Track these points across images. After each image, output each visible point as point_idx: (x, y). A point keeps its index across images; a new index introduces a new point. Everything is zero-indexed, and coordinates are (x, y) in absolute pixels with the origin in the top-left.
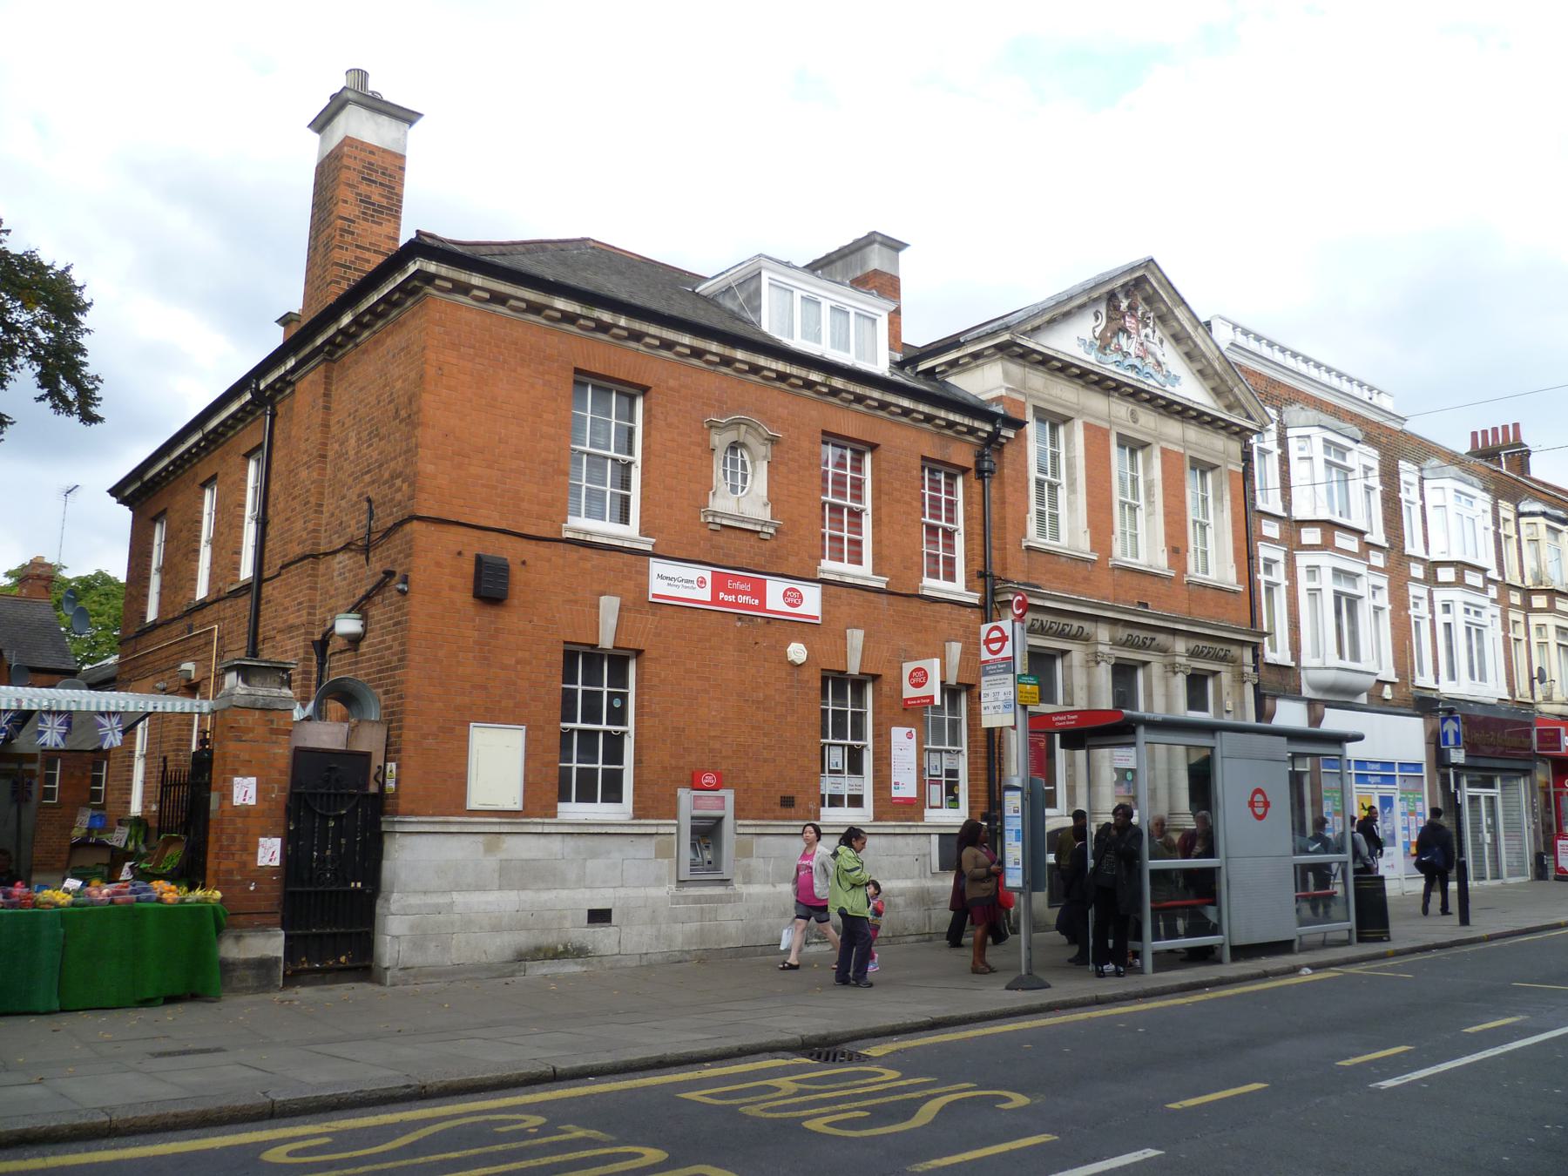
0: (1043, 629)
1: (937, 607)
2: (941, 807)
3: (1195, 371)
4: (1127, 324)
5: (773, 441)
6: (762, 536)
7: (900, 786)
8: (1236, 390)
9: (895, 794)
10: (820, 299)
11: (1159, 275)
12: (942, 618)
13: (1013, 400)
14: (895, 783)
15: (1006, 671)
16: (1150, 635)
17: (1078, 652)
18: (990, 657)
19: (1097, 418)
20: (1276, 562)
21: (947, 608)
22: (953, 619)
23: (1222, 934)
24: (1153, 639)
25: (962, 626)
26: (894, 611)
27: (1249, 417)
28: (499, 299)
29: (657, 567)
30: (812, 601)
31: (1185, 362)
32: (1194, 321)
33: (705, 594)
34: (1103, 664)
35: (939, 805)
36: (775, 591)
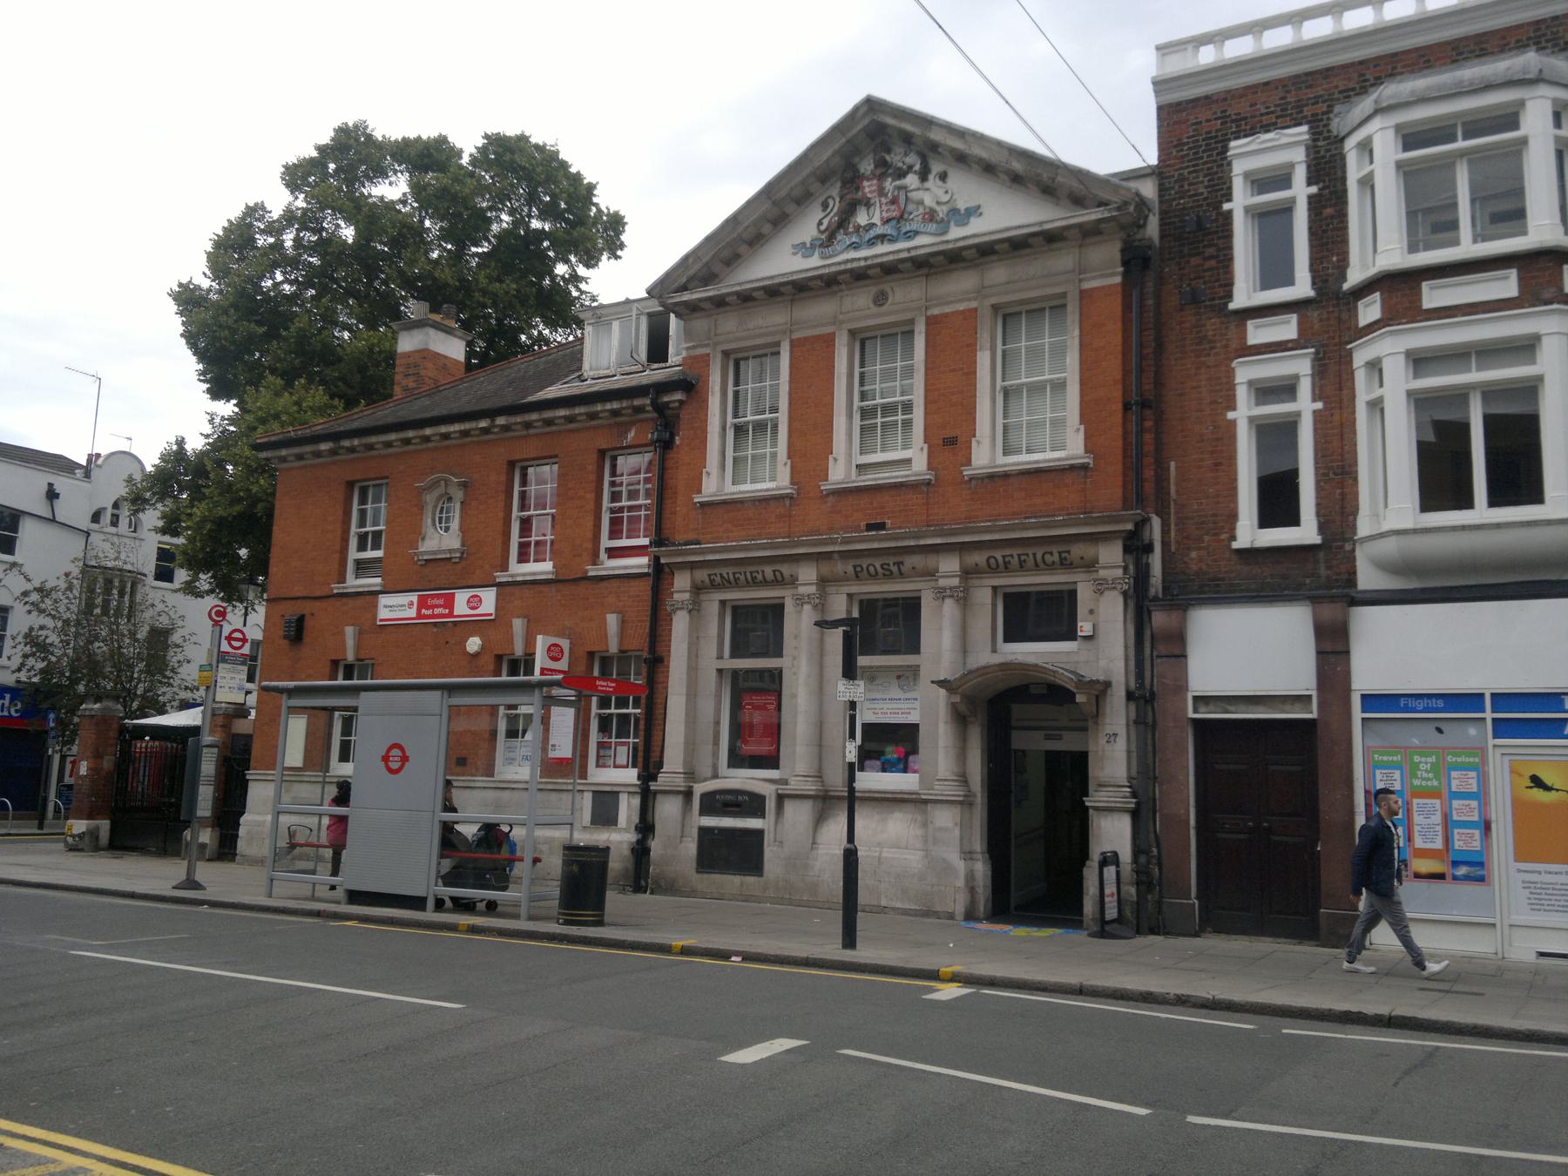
1: (605, 584)
2: (627, 767)
5: (464, 485)
6: (454, 560)
13: (695, 357)
14: (553, 746)
15: (243, 663)
18: (230, 650)
21: (615, 583)
27: (1102, 204)
29: (384, 600)
30: (488, 600)
33: (412, 613)
35: (625, 763)
36: (461, 599)
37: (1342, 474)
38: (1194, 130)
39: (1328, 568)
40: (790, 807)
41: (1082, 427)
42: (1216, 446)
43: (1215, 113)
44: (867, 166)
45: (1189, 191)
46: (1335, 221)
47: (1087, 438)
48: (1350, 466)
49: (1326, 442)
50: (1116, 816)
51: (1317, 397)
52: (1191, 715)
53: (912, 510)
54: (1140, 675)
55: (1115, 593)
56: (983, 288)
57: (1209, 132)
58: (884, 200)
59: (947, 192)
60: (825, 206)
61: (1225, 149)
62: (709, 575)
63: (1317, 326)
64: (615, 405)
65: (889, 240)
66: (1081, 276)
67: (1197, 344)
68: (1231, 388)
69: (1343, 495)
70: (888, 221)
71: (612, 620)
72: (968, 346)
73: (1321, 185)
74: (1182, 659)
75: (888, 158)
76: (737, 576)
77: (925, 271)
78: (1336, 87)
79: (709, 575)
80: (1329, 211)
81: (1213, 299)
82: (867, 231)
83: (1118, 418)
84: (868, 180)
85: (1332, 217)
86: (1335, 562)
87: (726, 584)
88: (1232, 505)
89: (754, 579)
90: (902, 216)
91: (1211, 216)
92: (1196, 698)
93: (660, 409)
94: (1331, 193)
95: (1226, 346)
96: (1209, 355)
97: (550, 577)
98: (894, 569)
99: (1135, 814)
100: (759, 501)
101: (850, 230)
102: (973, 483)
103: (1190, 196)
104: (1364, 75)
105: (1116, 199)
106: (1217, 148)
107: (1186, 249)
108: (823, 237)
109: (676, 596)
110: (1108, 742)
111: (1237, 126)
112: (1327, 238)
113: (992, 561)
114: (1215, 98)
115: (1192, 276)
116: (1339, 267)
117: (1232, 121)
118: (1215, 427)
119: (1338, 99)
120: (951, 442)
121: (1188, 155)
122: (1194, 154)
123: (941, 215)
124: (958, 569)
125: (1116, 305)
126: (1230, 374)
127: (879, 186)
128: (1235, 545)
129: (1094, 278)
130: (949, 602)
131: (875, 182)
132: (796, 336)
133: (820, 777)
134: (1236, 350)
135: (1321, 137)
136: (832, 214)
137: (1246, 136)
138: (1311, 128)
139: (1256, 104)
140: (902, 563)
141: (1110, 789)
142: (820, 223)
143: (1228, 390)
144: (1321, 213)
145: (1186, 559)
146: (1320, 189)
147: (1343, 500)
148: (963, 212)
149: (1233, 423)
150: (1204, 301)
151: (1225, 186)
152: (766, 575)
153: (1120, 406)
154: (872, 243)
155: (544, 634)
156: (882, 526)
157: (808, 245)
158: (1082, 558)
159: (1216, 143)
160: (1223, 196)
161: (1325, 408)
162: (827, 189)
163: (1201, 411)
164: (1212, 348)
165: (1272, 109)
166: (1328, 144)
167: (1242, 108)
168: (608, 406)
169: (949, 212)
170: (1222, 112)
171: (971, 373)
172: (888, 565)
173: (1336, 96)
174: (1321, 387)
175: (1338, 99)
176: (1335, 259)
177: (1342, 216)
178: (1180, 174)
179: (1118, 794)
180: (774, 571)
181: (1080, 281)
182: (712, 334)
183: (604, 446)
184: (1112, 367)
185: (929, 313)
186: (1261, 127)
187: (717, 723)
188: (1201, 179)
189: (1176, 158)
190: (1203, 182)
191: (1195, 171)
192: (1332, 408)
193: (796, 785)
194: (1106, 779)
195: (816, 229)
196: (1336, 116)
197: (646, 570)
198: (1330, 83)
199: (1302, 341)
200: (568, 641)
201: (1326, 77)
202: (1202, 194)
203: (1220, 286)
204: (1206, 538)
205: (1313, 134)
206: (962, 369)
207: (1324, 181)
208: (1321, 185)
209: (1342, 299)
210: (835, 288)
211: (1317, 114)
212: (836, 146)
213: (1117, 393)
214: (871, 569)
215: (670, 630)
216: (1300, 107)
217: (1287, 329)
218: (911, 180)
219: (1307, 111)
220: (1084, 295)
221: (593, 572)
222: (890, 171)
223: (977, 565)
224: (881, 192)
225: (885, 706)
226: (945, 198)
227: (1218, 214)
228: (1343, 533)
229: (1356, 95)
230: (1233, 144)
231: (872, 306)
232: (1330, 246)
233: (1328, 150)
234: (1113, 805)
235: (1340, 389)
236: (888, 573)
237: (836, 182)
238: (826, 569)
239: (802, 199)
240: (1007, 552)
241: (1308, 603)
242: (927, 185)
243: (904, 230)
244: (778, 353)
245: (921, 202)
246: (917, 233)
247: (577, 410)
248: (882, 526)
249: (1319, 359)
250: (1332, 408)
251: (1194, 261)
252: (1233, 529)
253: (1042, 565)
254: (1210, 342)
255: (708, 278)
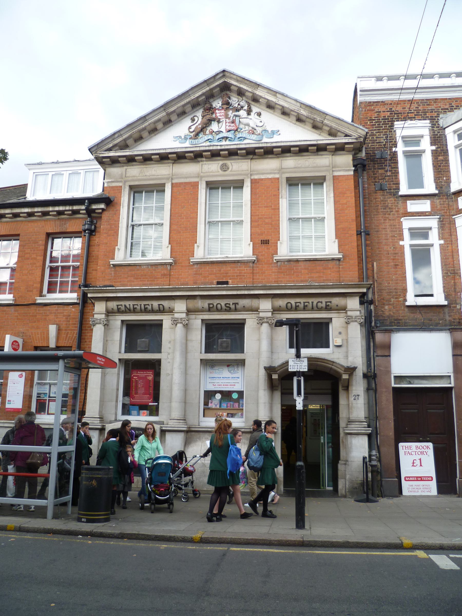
0: (130, 310)
1: (48, 308)
3: (295, 122)
4: (218, 115)
7: (12, 402)
8: (326, 121)
9: (8, 406)
10: (62, 172)
11: (235, 77)
12: (51, 313)
14: (8, 401)
16: (231, 301)
17: (167, 321)
19: (186, 178)
20: (430, 229)
21: (55, 308)
22: (58, 313)
23: (46, 499)
24: (235, 304)
25: (64, 316)
26: (18, 314)
27: (346, 136)
28: (16, 215)
31: (171, 127)
32: (272, 92)
34: (179, 325)
37: (454, 273)
38: (378, 115)
39: (450, 316)
40: (169, 436)
41: (337, 240)
42: (395, 257)
43: (387, 109)
44: (217, 104)
45: (377, 140)
46: (444, 162)
47: (340, 246)
48: (457, 270)
49: (446, 259)
50: (360, 437)
51: (441, 238)
52: (393, 385)
53: (244, 276)
54: (369, 366)
55: (356, 323)
56: (282, 168)
57: (385, 117)
58: (228, 120)
59: (261, 122)
60: (193, 120)
61: (392, 125)
62: (118, 306)
63: (439, 207)
64: (61, 208)
65: (229, 140)
66: (333, 169)
67: (384, 209)
68: (401, 230)
69: (455, 283)
70: (229, 131)
71: (53, 329)
72: (274, 195)
73: (437, 146)
74: (388, 357)
75: (229, 101)
76: (135, 306)
77: (251, 156)
78: (440, 107)
79: (118, 306)
80: (441, 158)
81: (391, 189)
82: (217, 134)
83: (355, 237)
84: (218, 109)
85: (442, 160)
86: (452, 314)
87: (128, 311)
88: (404, 285)
89: (146, 309)
90: (237, 130)
91: (387, 153)
92: (395, 377)
93: (90, 212)
94: (441, 150)
95: (398, 211)
96: (390, 214)
97: (11, 302)
98: (233, 307)
99: (370, 436)
100: (151, 265)
101: (207, 133)
102: (279, 263)
103: (377, 143)
104: (451, 104)
105: (355, 135)
106: (389, 124)
107: (376, 165)
108: (192, 134)
109: (96, 316)
110: (355, 399)
111: (397, 116)
112: (441, 169)
113: (289, 305)
114: (386, 102)
115: (380, 178)
116: (446, 182)
117: (395, 114)
118: (394, 248)
119: (441, 112)
120: (265, 242)
121: (375, 125)
122: (378, 125)
123: (259, 132)
124: (270, 308)
125: (351, 183)
126: (401, 224)
127: (225, 115)
128: (407, 304)
129: (340, 171)
130: (265, 326)
131: (223, 111)
132: (174, 181)
133: (185, 420)
134: (402, 214)
135: (435, 126)
136: (197, 124)
137: (401, 121)
138: (431, 122)
139: (405, 108)
140: (238, 304)
141: (357, 423)
142: (190, 128)
143: (400, 231)
144: (437, 158)
145: (382, 309)
146: (436, 148)
147: (455, 285)
148: (270, 132)
149: (403, 247)
150: (386, 190)
151: (393, 141)
152: (153, 306)
153: (355, 232)
154: (220, 139)
155: (11, 334)
156: (227, 283)
157: (183, 137)
158: (337, 306)
159: (388, 121)
160: (392, 144)
161: (445, 244)
162: (194, 112)
163: (387, 240)
164: (391, 212)
165: (413, 111)
166: (439, 130)
167: (399, 109)
168: (57, 208)
169: (262, 131)
170: (390, 109)
171: (277, 209)
172: (229, 304)
173: (440, 111)
174: (442, 234)
175: (441, 112)
176: (445, 178)
177: (447, 161)
178: (371, 133)
179: (360, 426)
180: (159, 305)
181: (333, 171)
182: (124, 176)
183: (50, 231)
184: (351, 213)
185: (252, 177)
186: (408, 118)
187: (118, 390)
188: (382, 136)
189: (369, 125)
190: (383, 137)
191: (378, 132)
192: (448, 244)
193: (172, 425)
194: (354, 418)
195: (188, 131)
196: (441, 118)
197: (76, 301)
198: (437, 105)
199: (432, 213)
200: (22, 340)
201: (435, 102)
202: (383, 142)
203: (393, 184)
204: (392, 300)
205: (432, 124)
206: (271, 206)
207: (438, 145)
208: (437, 146)
209: (449, 196)
210: (199, 159)
211: (433, 117)
212: (204, 91)
213: (354, 226)
214: (219, 306)
215: (92, 336)
216: (425, 113)
217: (426, 206)
218: (243, 113)
219: (428, 115)
220: (335, 178)
221: (40, 300)
222: (231, 107)
223: (280, 306)
224: (227, 117)
225: (220, 381)
226: (261, 124)
227: (390, 152)
228: (456, 301)
229: (448, 111)
230: (396, 123)
231: (220, 170)
232: (442, 173)
233: (439, 132)
234: (360, 431)
235: (451, 235)
236: (228, 309)
237: (201, 108)
238: (193, 304)
239: (182, 114)
240: (298, 300)
241: (448, 331)
242: (250, 117)
243: (238, 136)
244: (164, 191)
245: (248, 125)
246: (245, 138)
247: (36, 209)
248: (227, 283)
249: (441, 221)
250: (448, 244)
251: (380, 171)
252: (405, 296)
253: (315, 308)
254: (390, 208)
255: (124, 146)
